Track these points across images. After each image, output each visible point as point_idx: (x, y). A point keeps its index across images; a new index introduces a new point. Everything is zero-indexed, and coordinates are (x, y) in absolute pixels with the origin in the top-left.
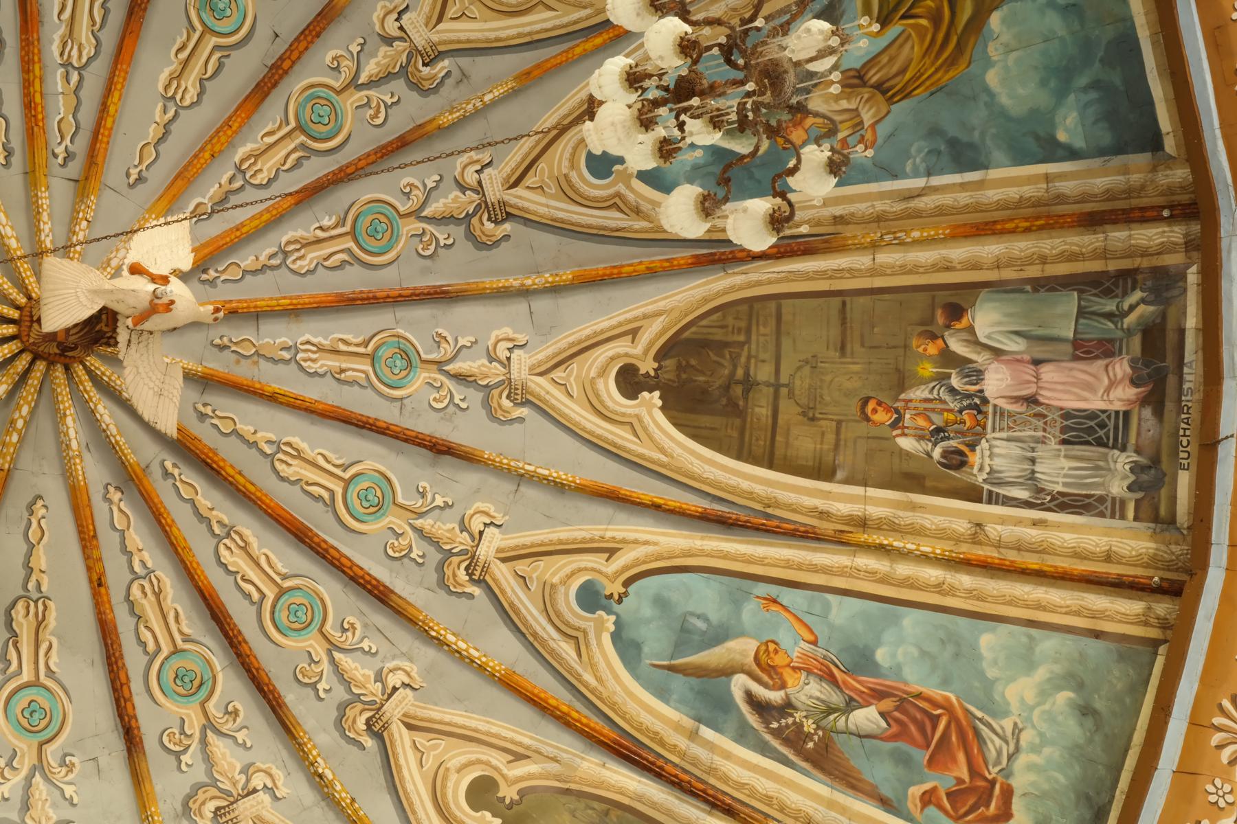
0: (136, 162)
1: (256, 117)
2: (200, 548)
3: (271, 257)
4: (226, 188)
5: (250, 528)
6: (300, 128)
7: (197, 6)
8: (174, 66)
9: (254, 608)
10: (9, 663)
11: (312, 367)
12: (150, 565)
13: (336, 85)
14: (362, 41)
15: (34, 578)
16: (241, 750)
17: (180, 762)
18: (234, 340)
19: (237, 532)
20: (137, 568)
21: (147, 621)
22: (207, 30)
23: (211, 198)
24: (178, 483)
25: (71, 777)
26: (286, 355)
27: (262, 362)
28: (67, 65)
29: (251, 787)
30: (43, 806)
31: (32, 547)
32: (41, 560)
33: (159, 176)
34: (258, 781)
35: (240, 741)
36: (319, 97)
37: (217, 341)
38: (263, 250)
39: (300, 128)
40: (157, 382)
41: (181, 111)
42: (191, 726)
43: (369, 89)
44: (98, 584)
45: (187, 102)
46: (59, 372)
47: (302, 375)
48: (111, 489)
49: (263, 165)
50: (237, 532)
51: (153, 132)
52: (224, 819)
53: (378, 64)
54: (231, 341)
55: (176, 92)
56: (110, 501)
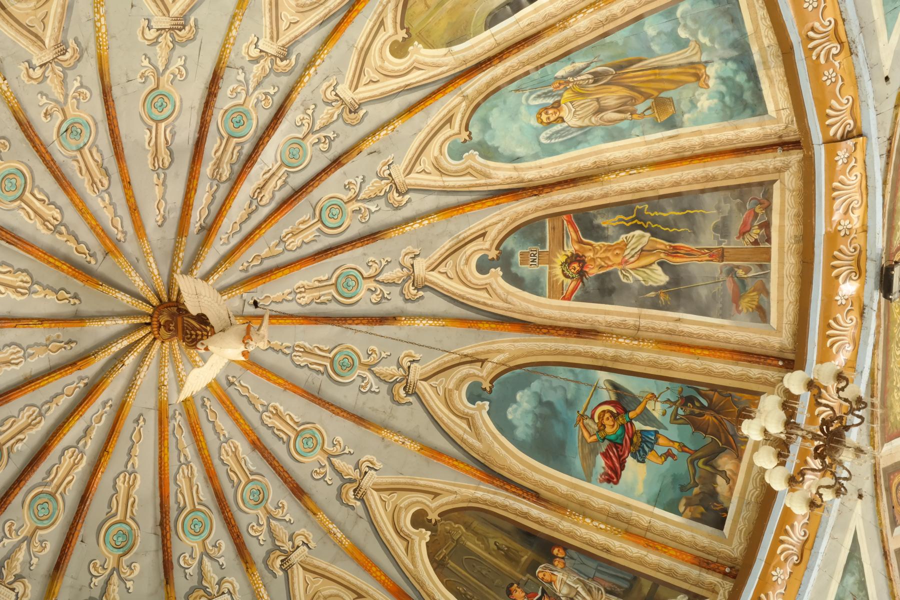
0: (142, 429)
1: (82, 488)
2: (72, 216)
3: (49, 409)
4: (88, 437)
5: (43, 236)
6: (53, 495)
7: (133, 531)
8: (133, 493)
9: (36, 184)
10: (170, 132)
11: (14, 349)
12: (99, 199)
13: (40, 532)
14: (32, 568)
15: (161, 181)
16: (45, 92)
17: (81, 83)
18: (63, 349)
19: (51, 230)
20: (106, 196)
21: (98, 165)
22: (123, 522)
23: (94, 428)
24: (87, 252)
25: (143, 71)
26: (30, 351)
27: (44, 342)
28: (187, 463)
29: (43, 68)
30: (162, 52)
31: (163, 197)
32: (158, 191)
33: (127, 425)
34: (38, 72)
35: (44, 97)
36: (47, 519)
37: (73, 345)
38: (54, 412)
39: (53, 495)
40: (203, 300)
41: (125, 469)
42: (72, 104)
43: (19, 541)
44: (127, 184)
45: (122, 475)
46: (165, 298)
47: (18, 342)
48: (123, 240)
49: (70, 461)
50: (51, 230)
51: (137, 450)
52: (62, 48)
53: (18, 559)
54: (65, 348)
55: (130, 478)
56: (123, 232)
